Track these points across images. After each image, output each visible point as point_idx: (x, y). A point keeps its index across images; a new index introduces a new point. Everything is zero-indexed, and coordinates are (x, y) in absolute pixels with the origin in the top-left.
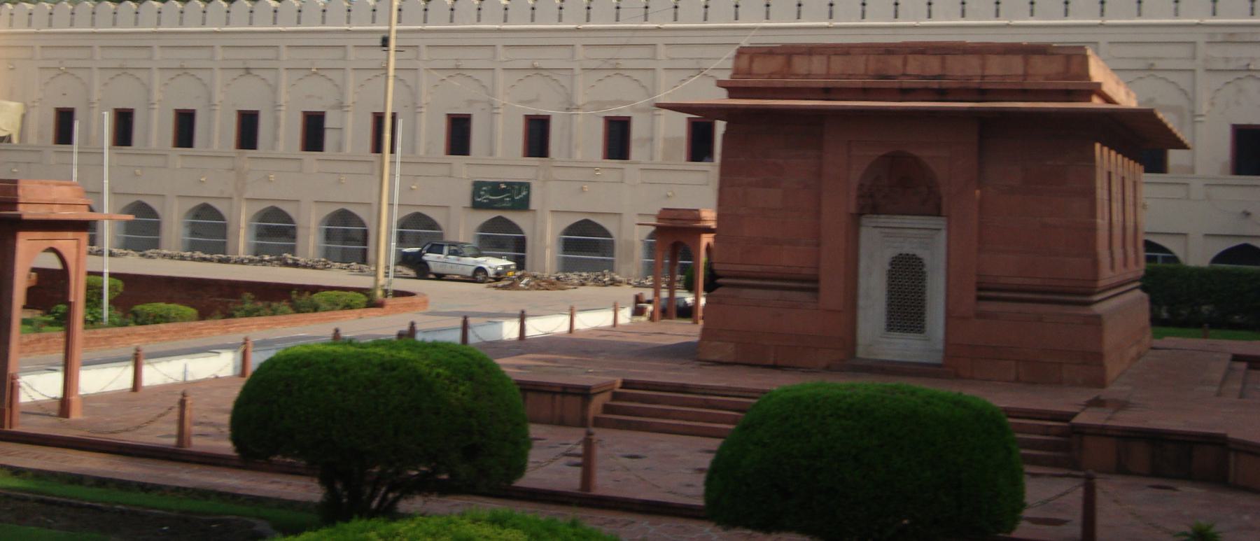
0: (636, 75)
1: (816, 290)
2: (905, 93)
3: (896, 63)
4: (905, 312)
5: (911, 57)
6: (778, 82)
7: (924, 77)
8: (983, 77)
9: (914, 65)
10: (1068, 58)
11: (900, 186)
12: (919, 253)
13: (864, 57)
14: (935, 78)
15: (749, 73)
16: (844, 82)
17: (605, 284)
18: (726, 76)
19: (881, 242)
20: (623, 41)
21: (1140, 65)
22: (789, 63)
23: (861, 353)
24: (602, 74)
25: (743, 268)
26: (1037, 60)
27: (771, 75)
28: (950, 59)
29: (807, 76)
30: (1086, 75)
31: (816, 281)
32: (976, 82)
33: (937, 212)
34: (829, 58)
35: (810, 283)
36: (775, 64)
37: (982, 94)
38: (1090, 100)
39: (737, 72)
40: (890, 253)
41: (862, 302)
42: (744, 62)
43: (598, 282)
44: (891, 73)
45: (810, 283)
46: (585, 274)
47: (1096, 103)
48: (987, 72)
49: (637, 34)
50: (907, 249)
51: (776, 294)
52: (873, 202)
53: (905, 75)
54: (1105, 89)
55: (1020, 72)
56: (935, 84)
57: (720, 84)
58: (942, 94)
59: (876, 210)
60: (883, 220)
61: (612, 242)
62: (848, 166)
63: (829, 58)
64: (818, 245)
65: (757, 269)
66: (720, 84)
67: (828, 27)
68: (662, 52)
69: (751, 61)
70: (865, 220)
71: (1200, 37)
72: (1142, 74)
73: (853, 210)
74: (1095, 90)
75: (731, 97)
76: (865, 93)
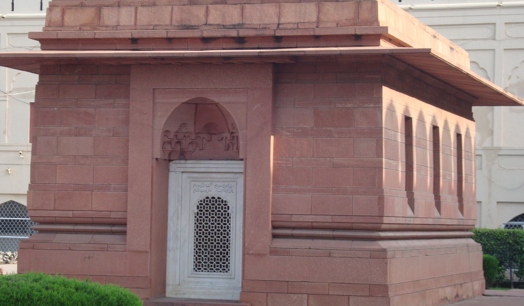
1: (124, 233)
2: (206, 41)
4: (211, 253)
5: (210, 6)
6: (87, 34)
7: (224, 27)
11: (203, 132)
13: (170, 8)
14: (234, 27)
15: (63, 26)
16: (151, 34)
18: (39, 28)
19: (189, 187)
22: (99, 14)
23: (170, 292)
25: (57, 214)
29: (117, 27)
30: (376, 20)
31: (125, 224)
34: (136, 9)
35: (118, 227)
37: (278, 40)
38: (379, 45)
39: (49, 24)
40: (197, 197)
41: (170, 244)
42: (57, 14)
44: (194, 23)
45: (118, 227)
46: (9, 253)
47: (384, 45)
48: (283, 20)
50: (213, 193)
51: (87, 238)
52: (177, 149)
54: (391, 32)
55: (314, 19)
57: (33, 36)
58: (240, 41)
59: (183, 156)
60: (191, 165)
63: (136, 9)
64: (126, 190)
65: (70, 214)
66: (33, 36)
70: (173, 166)
73: (158, 154)
74: (382, 34)
75: (43, 50)
76: (170, 42)
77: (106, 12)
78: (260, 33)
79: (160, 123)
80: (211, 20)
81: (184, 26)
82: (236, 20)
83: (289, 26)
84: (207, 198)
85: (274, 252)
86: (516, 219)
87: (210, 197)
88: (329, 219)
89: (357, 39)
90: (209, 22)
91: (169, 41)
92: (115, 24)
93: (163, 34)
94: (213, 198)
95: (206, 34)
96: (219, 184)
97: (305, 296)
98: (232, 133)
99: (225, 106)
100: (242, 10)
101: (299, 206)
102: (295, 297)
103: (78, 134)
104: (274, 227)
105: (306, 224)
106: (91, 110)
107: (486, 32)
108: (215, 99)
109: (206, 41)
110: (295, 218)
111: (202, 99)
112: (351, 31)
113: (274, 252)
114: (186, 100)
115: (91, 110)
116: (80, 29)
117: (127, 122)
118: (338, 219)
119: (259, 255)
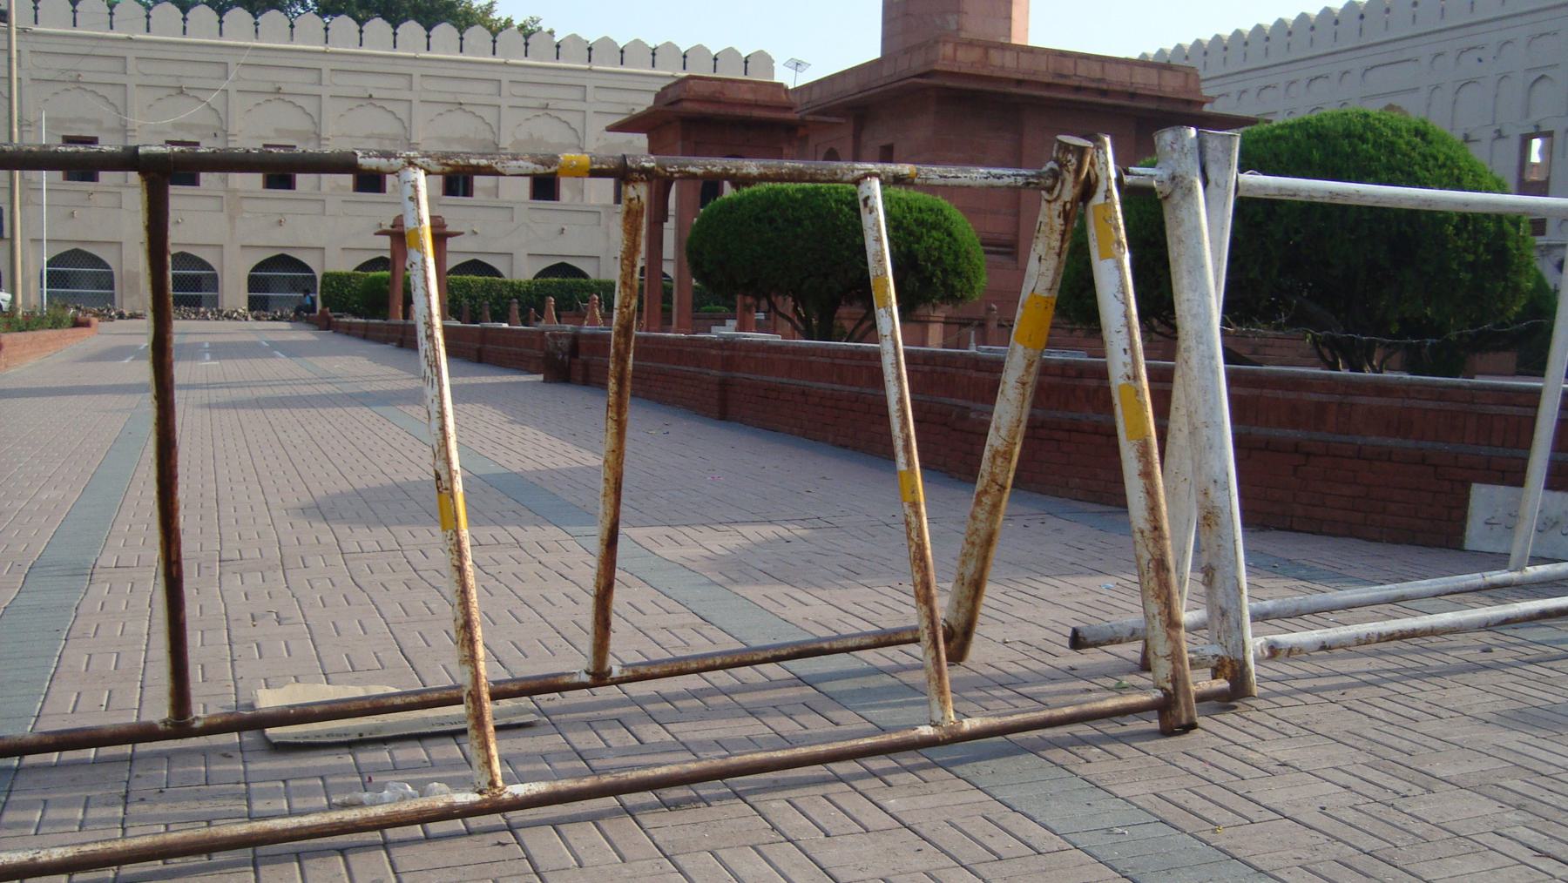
0: (101, 90)
3: (1069, 63)
9: (1082, 70)
17: (111, 319)
20: (85, 50)
24: (58, 87)
26: (1167, 75)
30: (1198, 90)
32: (1131, 90)
36: (975, 54)
37: (1133, 96)
43: (104, 316)
44: (1065, 72)
49: (103, 43)
56: (1094, 85)
61: (111, 275)
64: (1017, 214)
67: (325, 52)
68: (131, 63)
69: (955, 51)
77: (992, 52)
82: (1098, 75)
89: (1189, 102)
91: (1048, 86)
93: (1049, 79)
95: (1084, 84)
107: (577, 94)
109: (1078, 89)
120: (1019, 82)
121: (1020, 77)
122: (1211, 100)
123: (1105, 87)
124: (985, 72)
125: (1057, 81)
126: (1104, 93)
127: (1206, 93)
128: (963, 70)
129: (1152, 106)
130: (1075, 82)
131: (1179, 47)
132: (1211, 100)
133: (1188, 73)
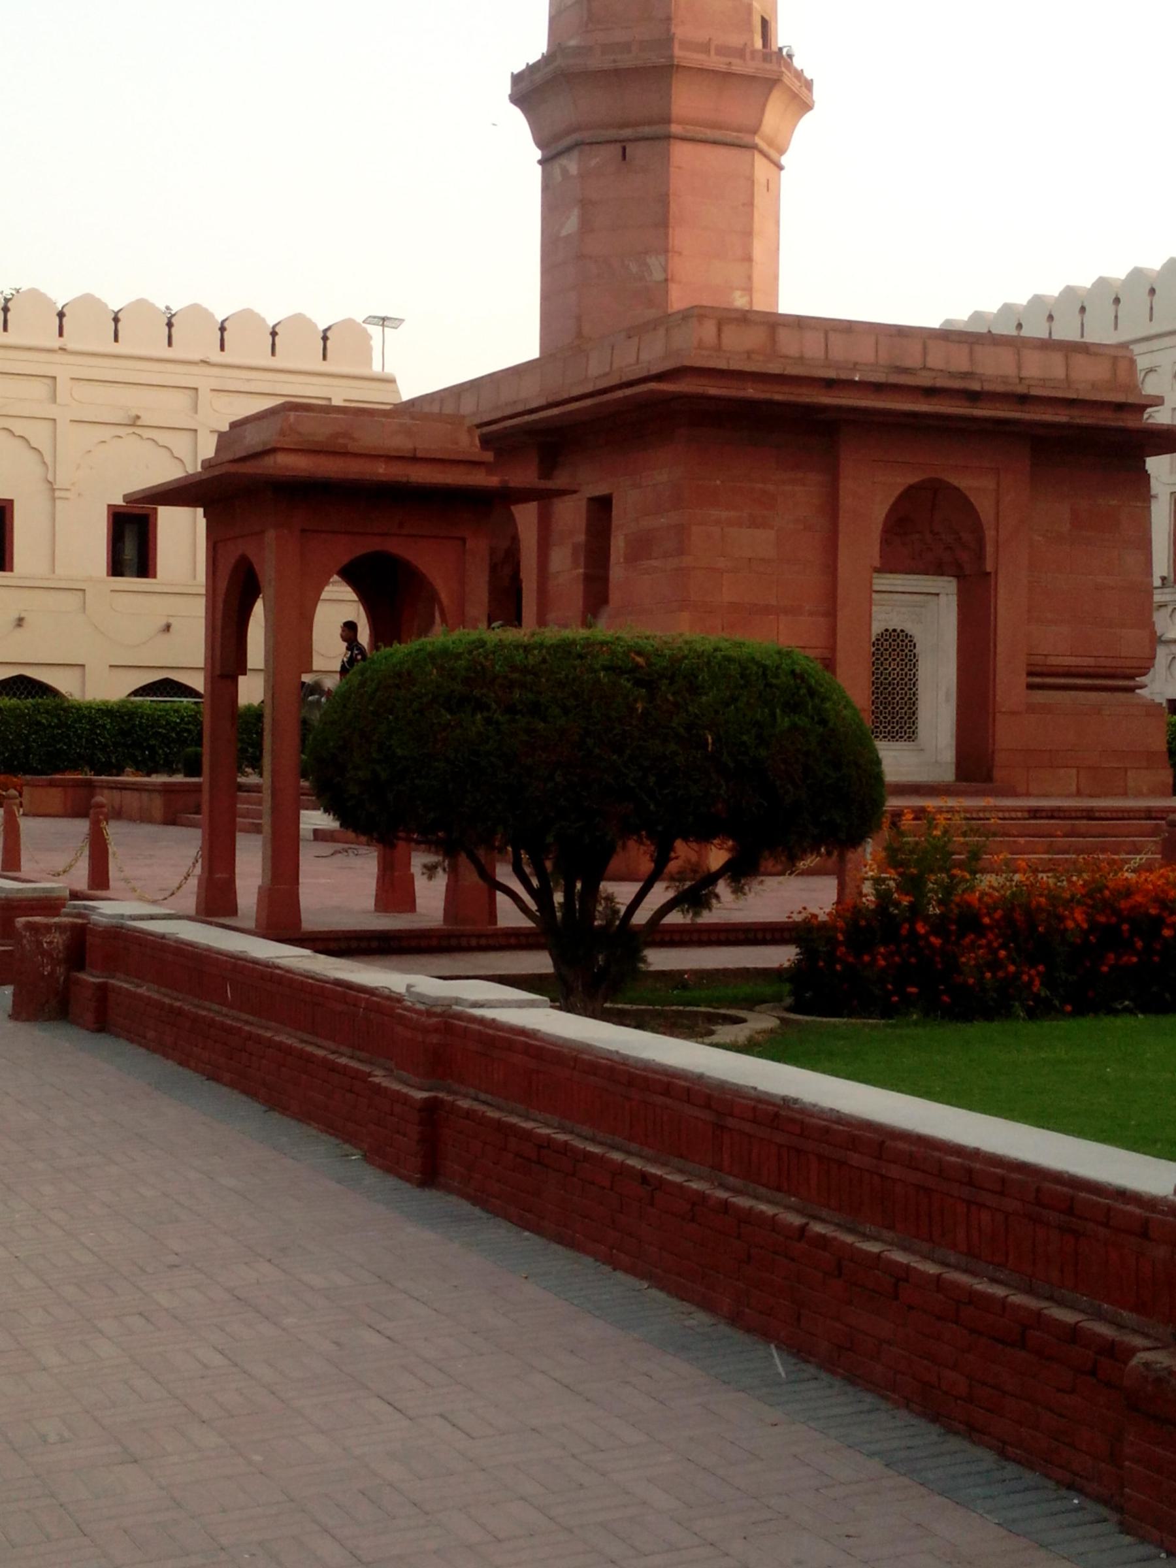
8: (1021, 379)
9: (936, 360)
10: (1115, 359)
12: (909, 628)
15: (719, 348)
21: (119, 417)
26: (1079, 359)
27: (749, 354)
28: (977, 348)
29: (801, 358)
32: (1021, 389)
33: (938, 569)
36: (753, 338)
37: (1024, 399)
44: (908, 363)
48: (1024, 374)
53: (925, 368)
55: (1063, 376)
56: (957, 384)
62: (871, 491)
63: (826, 333)
64: (831, 614)
69: (719, 330)
71: (204, 380)
72: (121, 431)
78: (1009, 389)
79: (879, 512)
80: (930, 363)
81: (897, 367)
82: (965, 367)
83: (1033, 383)
84: (887, 630)
85: (1031, 708)
86: (136, 693)
87: (891, 629)
88: (1091, 661)
89: (1120, 407)
90: (929, 365)
91: (878, 388)
92: (797, 355)
94: (894, 630)
95: (941, 383)
96: (903, 610)
97: (1074, 771)
98: (938, 534)
99: (967, 493)
100: (971, 352)
101: (1058, 644)
102: (1062, 771)
103: (754, 523)
104: (1030, 674)
105: (1060, 670)
106: (771, 487)
107: (39, 389)
108: (956, 483)
109: (930, 392)
110: (1053, 661)
111: (940, 481)
112: (1120, 398)
113: (1031, 708)
114: (912, 479)
115: (771, 487)
116: (749, 358)
117: (831, 507)
118: (1103, 662)
119: (1013, 713)
120: (830, 384)
121: (832, 374)
122: (1158, 401)
123: (976, 386)
124: (774, 368)
125: (894, 379)
126: (974, 397)
127: (1150, 387)
128: (734, 366)
129: (1061, 417)
130: (924, 380)
131: (1007, 308)
132: (1158, 401)
133: (1119, 357)
